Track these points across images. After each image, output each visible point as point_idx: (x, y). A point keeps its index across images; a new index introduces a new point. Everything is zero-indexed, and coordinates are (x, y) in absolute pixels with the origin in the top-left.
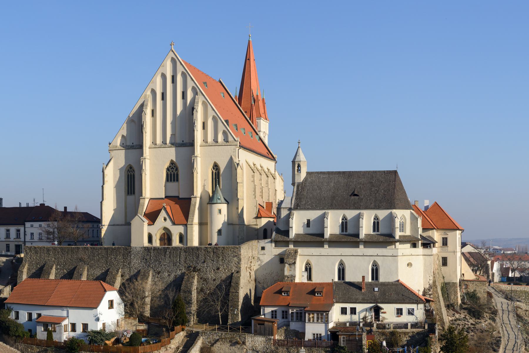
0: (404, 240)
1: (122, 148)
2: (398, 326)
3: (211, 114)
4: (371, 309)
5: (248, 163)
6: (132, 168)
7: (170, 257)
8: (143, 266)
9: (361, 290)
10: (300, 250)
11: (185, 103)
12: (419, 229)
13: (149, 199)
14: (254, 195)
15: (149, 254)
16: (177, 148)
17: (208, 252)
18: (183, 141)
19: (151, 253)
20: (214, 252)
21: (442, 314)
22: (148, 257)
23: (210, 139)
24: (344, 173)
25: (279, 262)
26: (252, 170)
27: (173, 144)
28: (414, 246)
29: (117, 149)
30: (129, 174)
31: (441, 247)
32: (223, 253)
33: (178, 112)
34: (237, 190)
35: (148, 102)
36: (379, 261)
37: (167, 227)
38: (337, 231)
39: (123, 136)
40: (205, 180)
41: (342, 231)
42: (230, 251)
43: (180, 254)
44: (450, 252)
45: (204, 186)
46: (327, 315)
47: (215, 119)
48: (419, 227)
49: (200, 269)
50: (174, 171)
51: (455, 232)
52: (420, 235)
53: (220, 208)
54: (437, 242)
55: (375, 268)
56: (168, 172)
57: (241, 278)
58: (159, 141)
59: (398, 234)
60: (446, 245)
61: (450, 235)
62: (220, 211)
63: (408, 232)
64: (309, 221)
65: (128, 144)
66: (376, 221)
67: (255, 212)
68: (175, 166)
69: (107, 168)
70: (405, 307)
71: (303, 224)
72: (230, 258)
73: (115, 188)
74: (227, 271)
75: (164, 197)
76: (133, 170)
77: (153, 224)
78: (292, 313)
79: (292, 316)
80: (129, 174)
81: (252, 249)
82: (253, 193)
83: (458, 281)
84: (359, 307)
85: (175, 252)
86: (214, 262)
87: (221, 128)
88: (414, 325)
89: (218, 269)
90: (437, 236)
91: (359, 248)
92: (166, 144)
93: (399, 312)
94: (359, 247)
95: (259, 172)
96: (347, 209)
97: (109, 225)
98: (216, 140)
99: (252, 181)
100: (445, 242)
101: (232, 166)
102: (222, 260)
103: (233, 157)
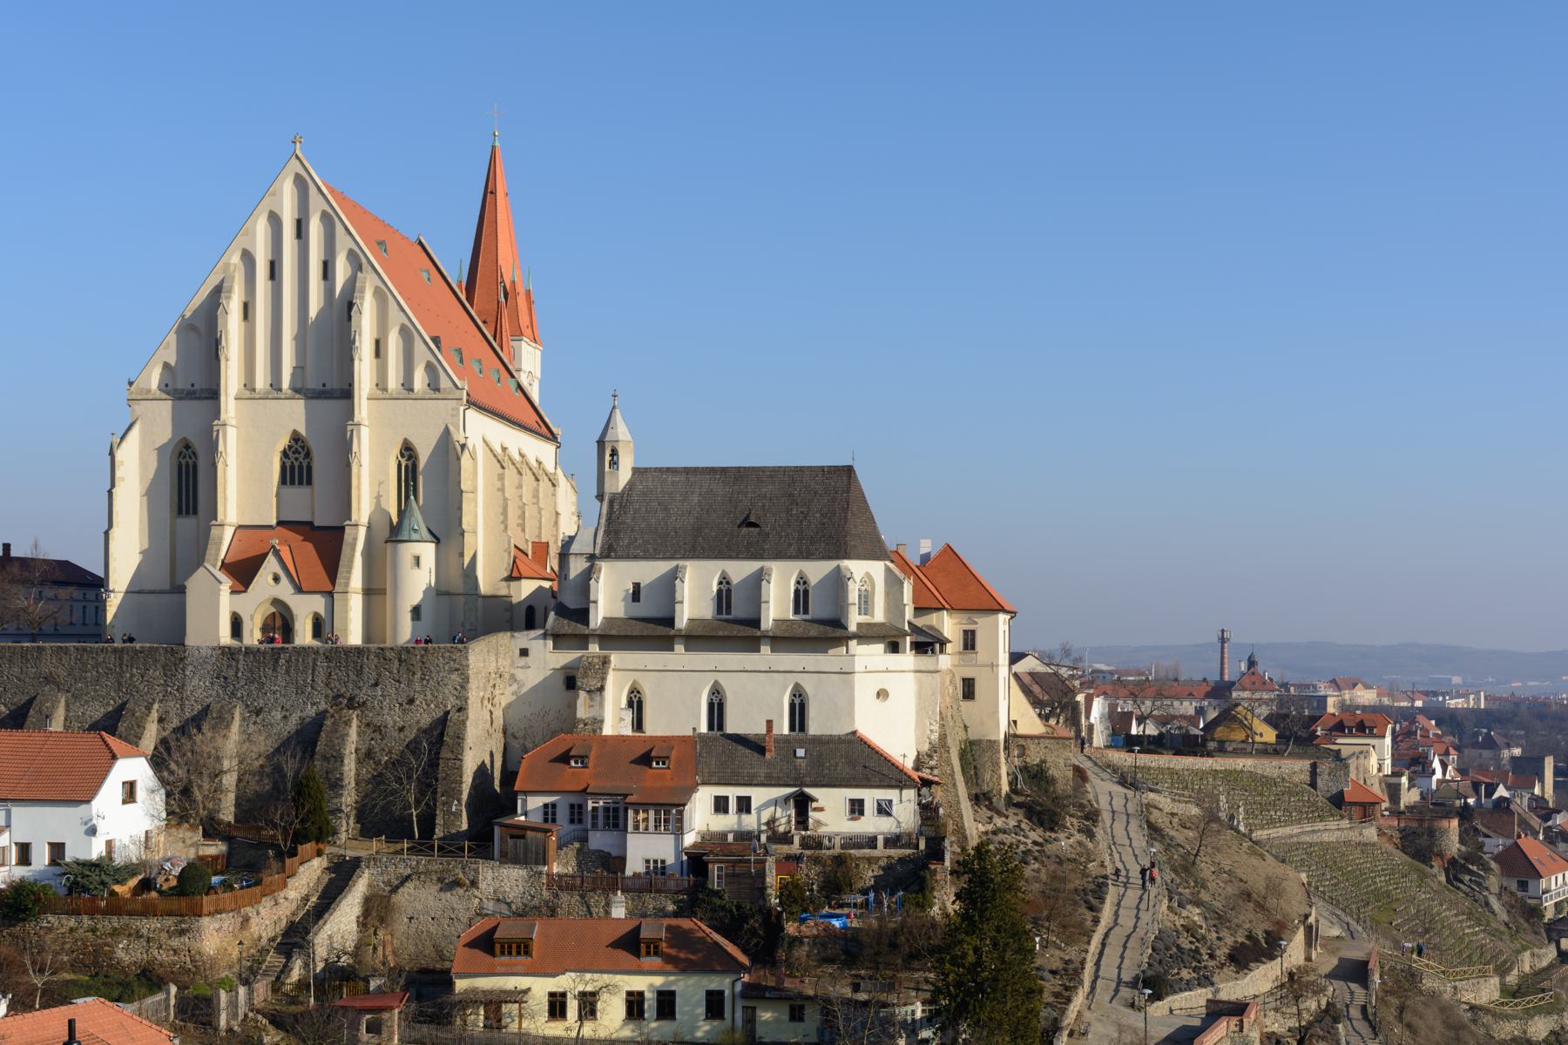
0: (868, 634)
1: (164, 396)
2: (853, 842)
3: (395, 319)
4: (786, 799)
5: (487, 445)
7: (287, 672)
8: (218, 696)
9: (764, 755)
10: (616, 658)
11: (329, 291)
12: (907, 608)
13: (233, 528)
14: (503, 522)
15: (234, 664)
16: (309, 401)
17: (385, 659)
18: (324, 385)
19: (237, 661)
20: (400, 660)
21: (961, 817)
22: (231, 673)
23: (394, 381)
24: (724, 470)
25: (564, 687)
26: (499, 461)
27: (299, 390)
28: (894, 648)
29: (151, 397)
30: (184, 462)
31: (960, 653)
32: (423, 663)
33: (313, 311)
34: (460, 508)
35: (233, 281)
36: (809, 685)
37: (281, 598)
38: (707, 611)
39: (166, 366)
40: (380, 484)
41: (719, 610)
42: (442, 656)
43: (315, 664)
44: (979, 666)
45: (378, 497)
46: (681, 813)
47: (406, 333)
48: (905, 602)
49: (364, 703)
50: (301, 460)
51: (994, 616)
52: (909, 623)
53: (417, 553)
54: (950, 642)
55: (797, 701)
56: (286, 460)
57: (468, 723)
58: (262, 381)
59: (854, 620)
60: (973, 647)
61: (982, 624)
62: (417, 560)
63: (879, 615)
64: (637, 586)
65: (180, 386)
66: (801, 588)
67: (505, 565)
68: (303, 447)
69: (124, 445)
70: (870, 796)
71: (624, 594)
72: (441, 675)
73: (145, 498)
74: (432, 706)
75: (274, 522)
76: (194, 454)
77: (245, 591)
78: (595, 809)
79: (595, 817)
80: (184, 462)
81: (496, 655)
82: (502, 518)
83: (1002, 737)
84: (759, 795)
86: (402, 685)
87: (421, 355)
88: (892, 841)
89: (411, 701)
90: (949, 625)
91: (759, 651)
92: (280, 390)
93: (857, 808)
94: (758, 651)
95: (517, 468)
96: (730, 558)
97: (127, 592)
98: (408, 385)
99: (499, 490)
100: (969, 641)
101: (449, 451)
102: (422, 679)
103: (451, 428)
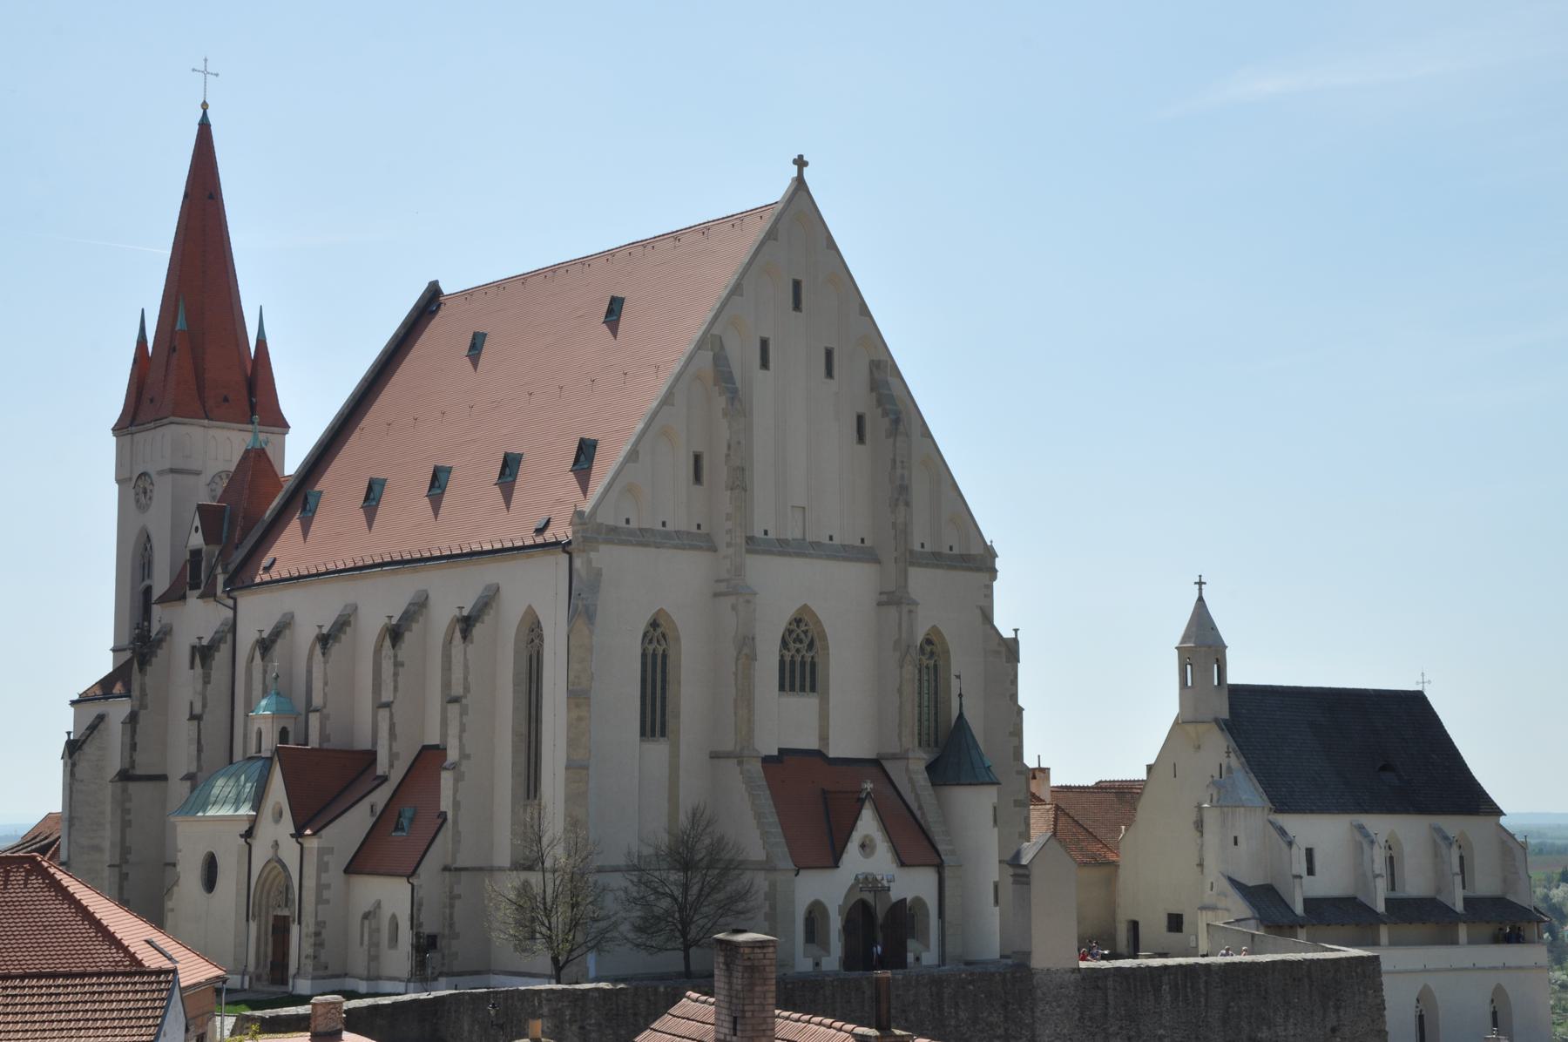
6: (658, 626)
56: (786, 652)
76: (664, 636)
85: (1189, 985)
96: (1366, 812)
